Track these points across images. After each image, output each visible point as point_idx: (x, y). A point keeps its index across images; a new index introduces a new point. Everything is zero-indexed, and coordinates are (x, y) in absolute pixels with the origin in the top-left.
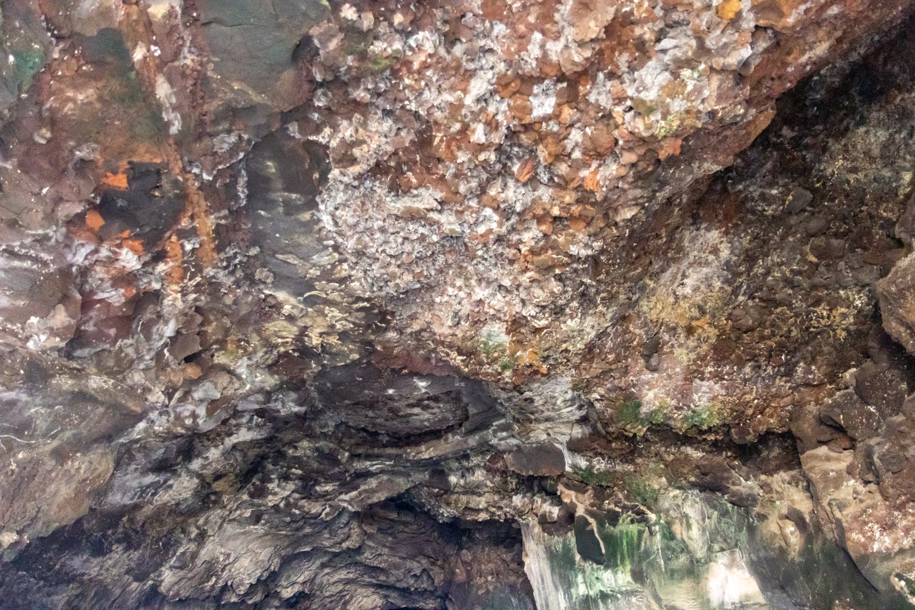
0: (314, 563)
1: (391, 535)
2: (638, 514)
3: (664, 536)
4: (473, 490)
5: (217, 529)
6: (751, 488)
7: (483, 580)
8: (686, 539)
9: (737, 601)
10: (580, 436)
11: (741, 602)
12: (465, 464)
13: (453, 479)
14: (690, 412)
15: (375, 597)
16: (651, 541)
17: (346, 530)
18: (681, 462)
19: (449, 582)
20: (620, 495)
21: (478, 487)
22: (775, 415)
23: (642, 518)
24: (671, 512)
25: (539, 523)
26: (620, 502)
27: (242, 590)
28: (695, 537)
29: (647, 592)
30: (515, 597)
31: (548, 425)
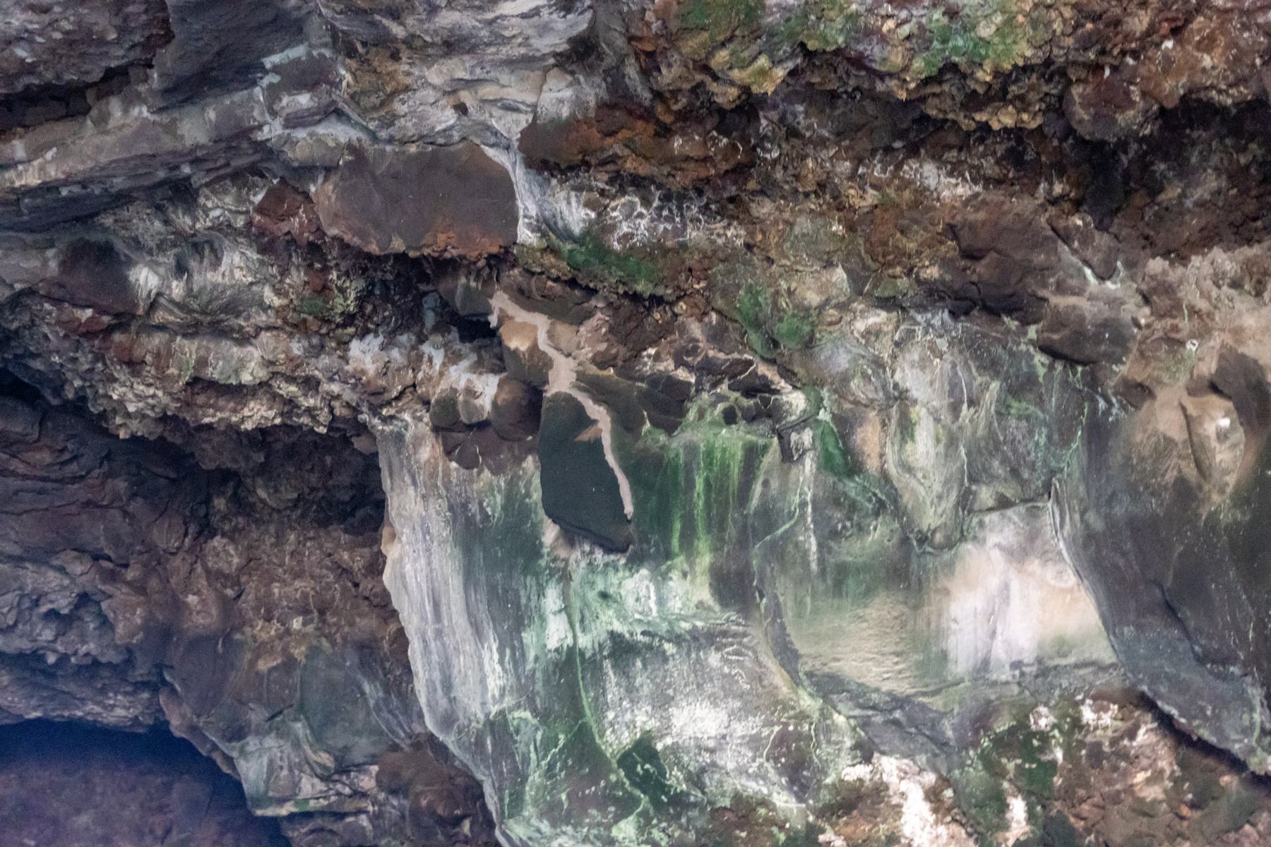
2: (749, 392)
3: (826, 463)
4: (216, 319)
6: (1114, 302)
7: (275, 628)
8: (893, 470)
9: (1028, 657)
10: (565, 112)
11: (1039, 661)
12: (184, 221)
13: (145, 278)
14: (937, 15)
16: (785, 475)
18: (901, 215)
19: (163, 635)
20: (696, 330)
21: (233, 307)
22: (1222, 41)
23: (759, 405)
24: (854, 384)
25: (436, 429)
26: (694, 351)
28: (921, 462)
29: (757, 635)
30: (373, 677)
31: (459, 68)
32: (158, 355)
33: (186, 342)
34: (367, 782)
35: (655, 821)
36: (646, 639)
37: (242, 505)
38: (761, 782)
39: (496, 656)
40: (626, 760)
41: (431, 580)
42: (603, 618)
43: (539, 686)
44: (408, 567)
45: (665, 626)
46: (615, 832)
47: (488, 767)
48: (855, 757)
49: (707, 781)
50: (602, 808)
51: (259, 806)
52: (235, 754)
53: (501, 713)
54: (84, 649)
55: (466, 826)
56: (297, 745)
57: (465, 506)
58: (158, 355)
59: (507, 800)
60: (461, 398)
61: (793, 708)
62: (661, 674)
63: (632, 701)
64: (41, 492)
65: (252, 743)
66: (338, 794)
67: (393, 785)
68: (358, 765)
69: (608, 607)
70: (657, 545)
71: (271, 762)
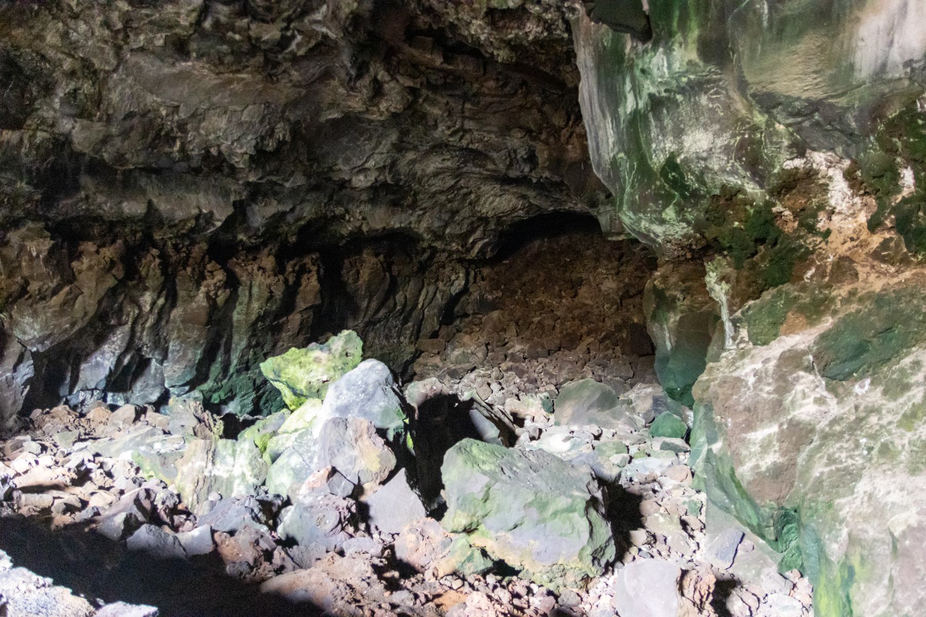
0: (379, 143)
1: (465, 98)
5: (114, 62)
17: (366, 81)
40: (664, 172)
43: (625, 137)
46: (664, 215)
48: (792, 153)
50: (655, 202)
53: (614, 157)
54: (544, 176)
61: (749, 123)
65: (602, 209)
71: (611, 217)
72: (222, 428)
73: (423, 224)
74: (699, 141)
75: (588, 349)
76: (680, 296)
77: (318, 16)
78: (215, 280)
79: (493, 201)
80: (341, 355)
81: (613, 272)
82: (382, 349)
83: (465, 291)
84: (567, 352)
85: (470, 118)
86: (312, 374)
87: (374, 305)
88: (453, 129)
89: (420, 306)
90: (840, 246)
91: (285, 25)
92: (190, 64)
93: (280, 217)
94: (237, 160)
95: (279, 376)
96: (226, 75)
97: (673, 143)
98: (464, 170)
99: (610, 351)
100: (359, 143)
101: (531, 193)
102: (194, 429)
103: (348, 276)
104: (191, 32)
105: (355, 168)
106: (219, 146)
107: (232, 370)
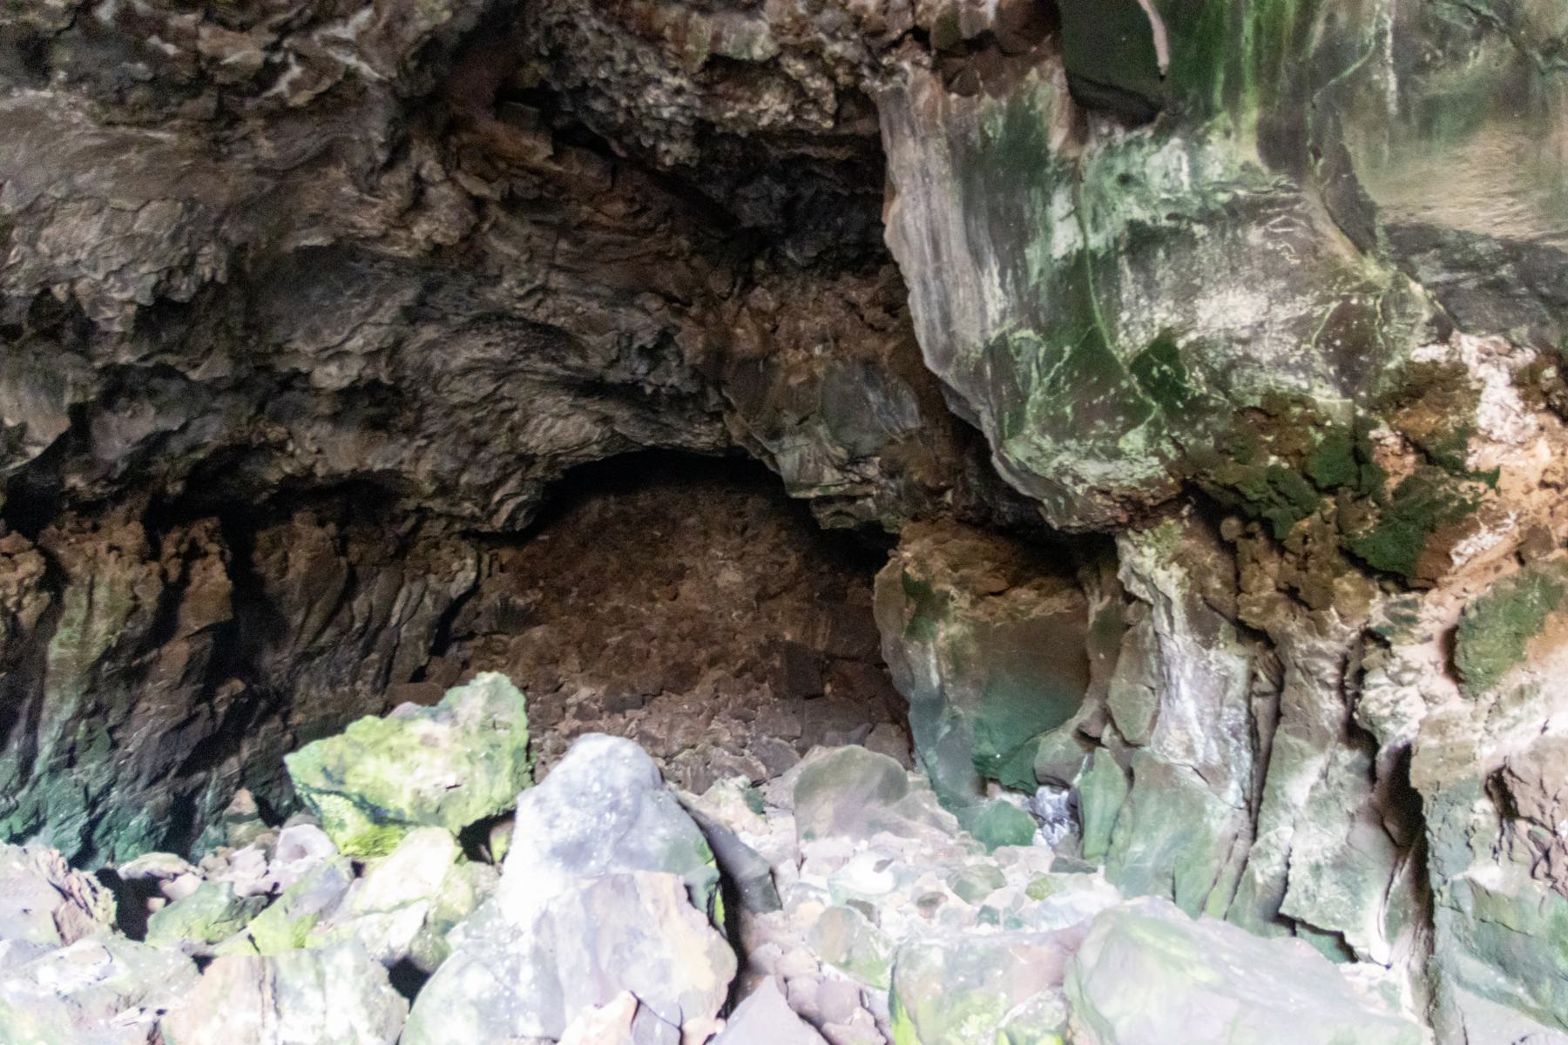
0: (378, 304)
1: (562, 230)
15: (579, 418)
17: (402, 175)
19: (719, 356)
27: (113, 320)
29: (1311, 200)
30: (874, 385)
32: (675, 27)
33: (701, 20)
34: (872, 471)
35: (1165, 432)
36: (1172, 224)
37: (776, 266)
38: (1301, 375)
39: (997, 280)
40: (1141, 364)
41: (930, 222)
42: (1120, 208)
43: (1044, 300)
44: (908, 218)
45: (1197, 202)
46: (1122, 444)
47: (986, 395)
48: (1430, 335)
49: (1234, 379)
50: (1110, 419)
51: (793, 490)
52: (775, 451)
53: (1002, 337)
54: (670, 382)
55: (949, 497)
56: (819, 442)
57: (965, 137)
58: (675, 27)
59: (1007, 421)
60: (963, 10)
61: (1357, 279)
62: (1187, 261)
63: (1151, 298)
64: (623, 245)
65: (787, 441)
66: (852, 482)
67: (892, 471)
68: (864, 457)
69: (1128, 192)
70: (1195, 103)
71: (801, 457)
72: (113, 906)
73: (419, 462)
74: (1229, 310)
75: (716, 690)
76: (953, 591)
77: (345, 32)
78: (21, 572)
79: (552, 427)
80: (483, 728)
81: (734, 555)
82: (323, 705)
83: (474, 590)
84: (674, 697)
85: (560, 269)
86: (420, 773)
87: (314, 621)
88: (528, 287)
89: (394, 621)
90: (1524, 497)
91: (273, 38)
92: (47, 94)
93: (156, 443)
94: (110, 314)
95: (342, 782)
96: (122, 129)
97: (1170, 311)
98: (521, 365)
99: (754, 693)
100: (341, 301)
101: (622, 413)
102: (54, 915)
103: (266, 567)
104: (62, 25)
105: (327, 349)
106: (72, 282)
107: (38, 767)
